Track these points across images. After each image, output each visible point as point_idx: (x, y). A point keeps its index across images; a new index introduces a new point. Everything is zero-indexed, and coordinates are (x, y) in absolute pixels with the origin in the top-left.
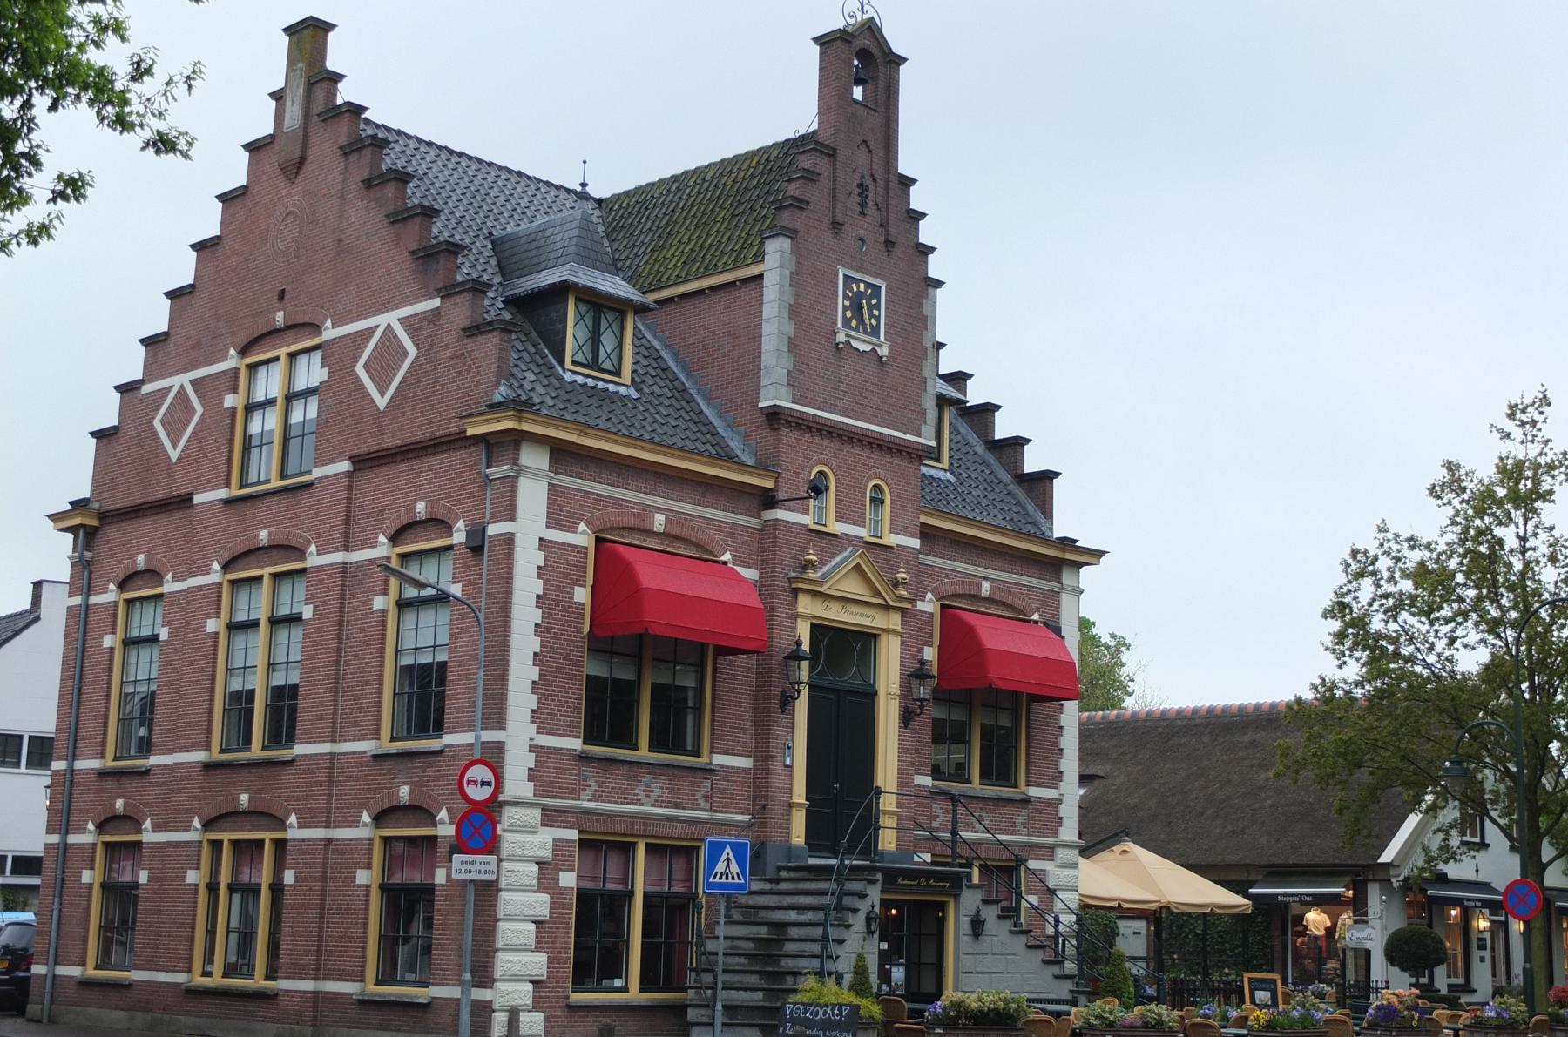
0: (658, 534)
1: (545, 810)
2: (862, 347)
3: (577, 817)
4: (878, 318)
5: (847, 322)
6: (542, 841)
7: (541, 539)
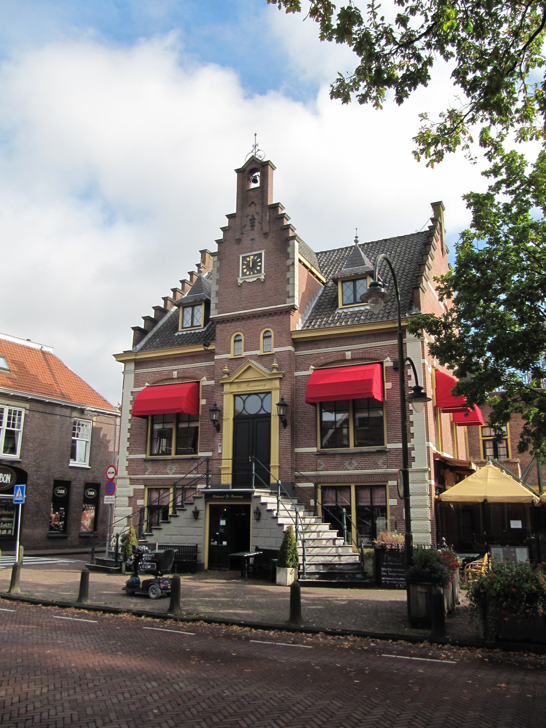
0: (176, 378)
1: (130, 479)
2: (251, 280)
3: (145, 482)
4: (260, 266)
5: (244, 274)
6: (130, 490)
7: (132, 392)
